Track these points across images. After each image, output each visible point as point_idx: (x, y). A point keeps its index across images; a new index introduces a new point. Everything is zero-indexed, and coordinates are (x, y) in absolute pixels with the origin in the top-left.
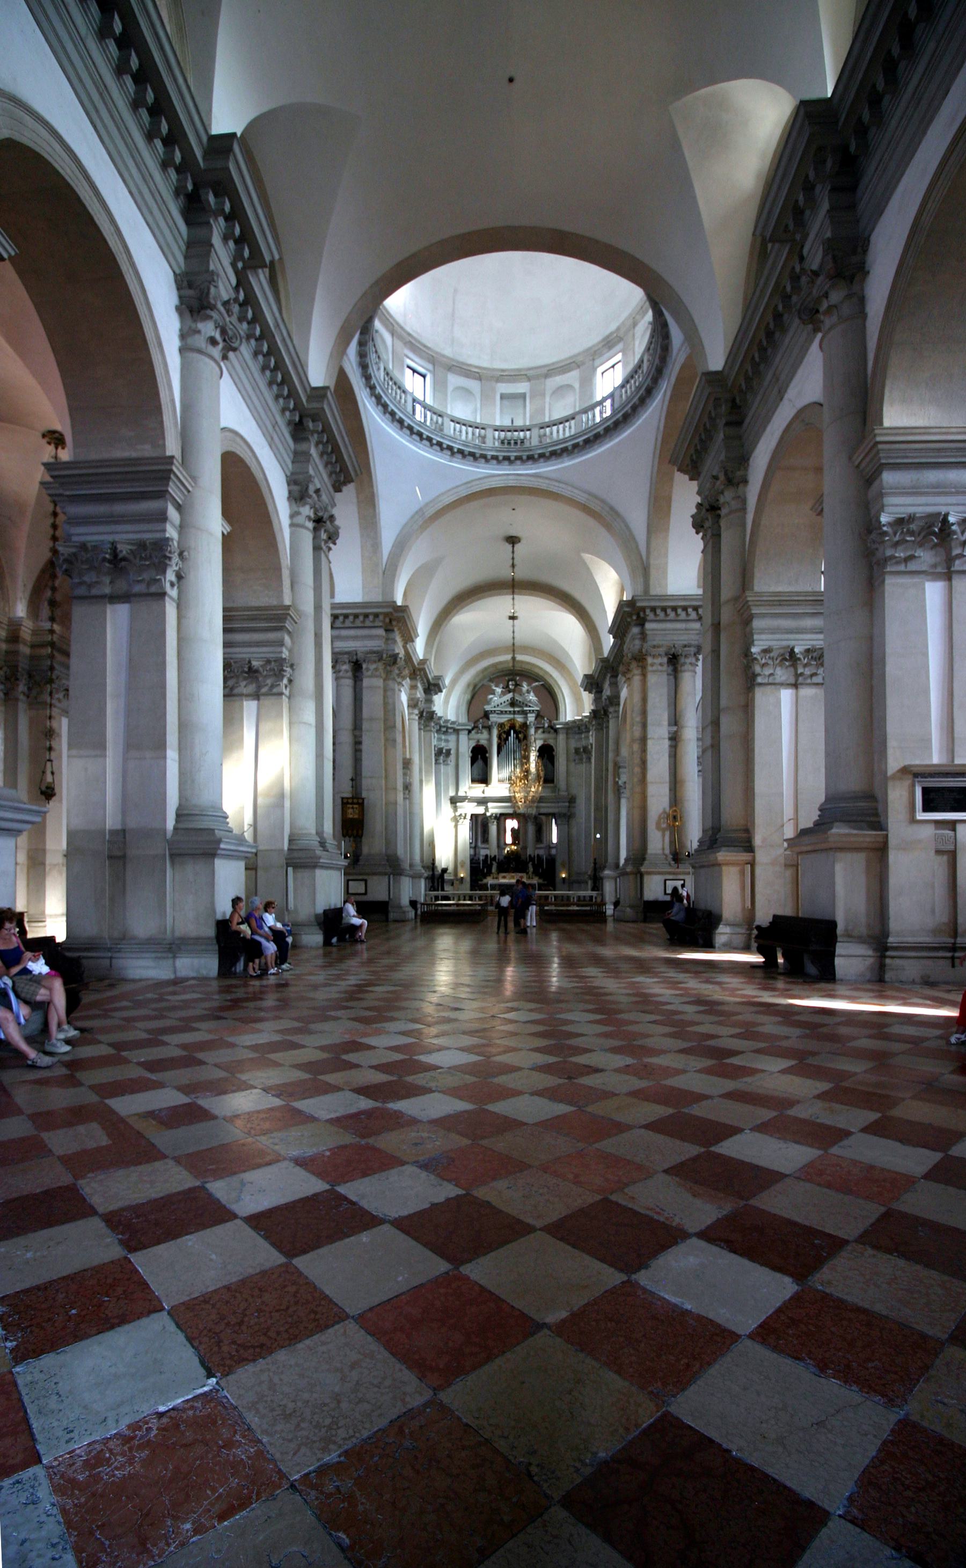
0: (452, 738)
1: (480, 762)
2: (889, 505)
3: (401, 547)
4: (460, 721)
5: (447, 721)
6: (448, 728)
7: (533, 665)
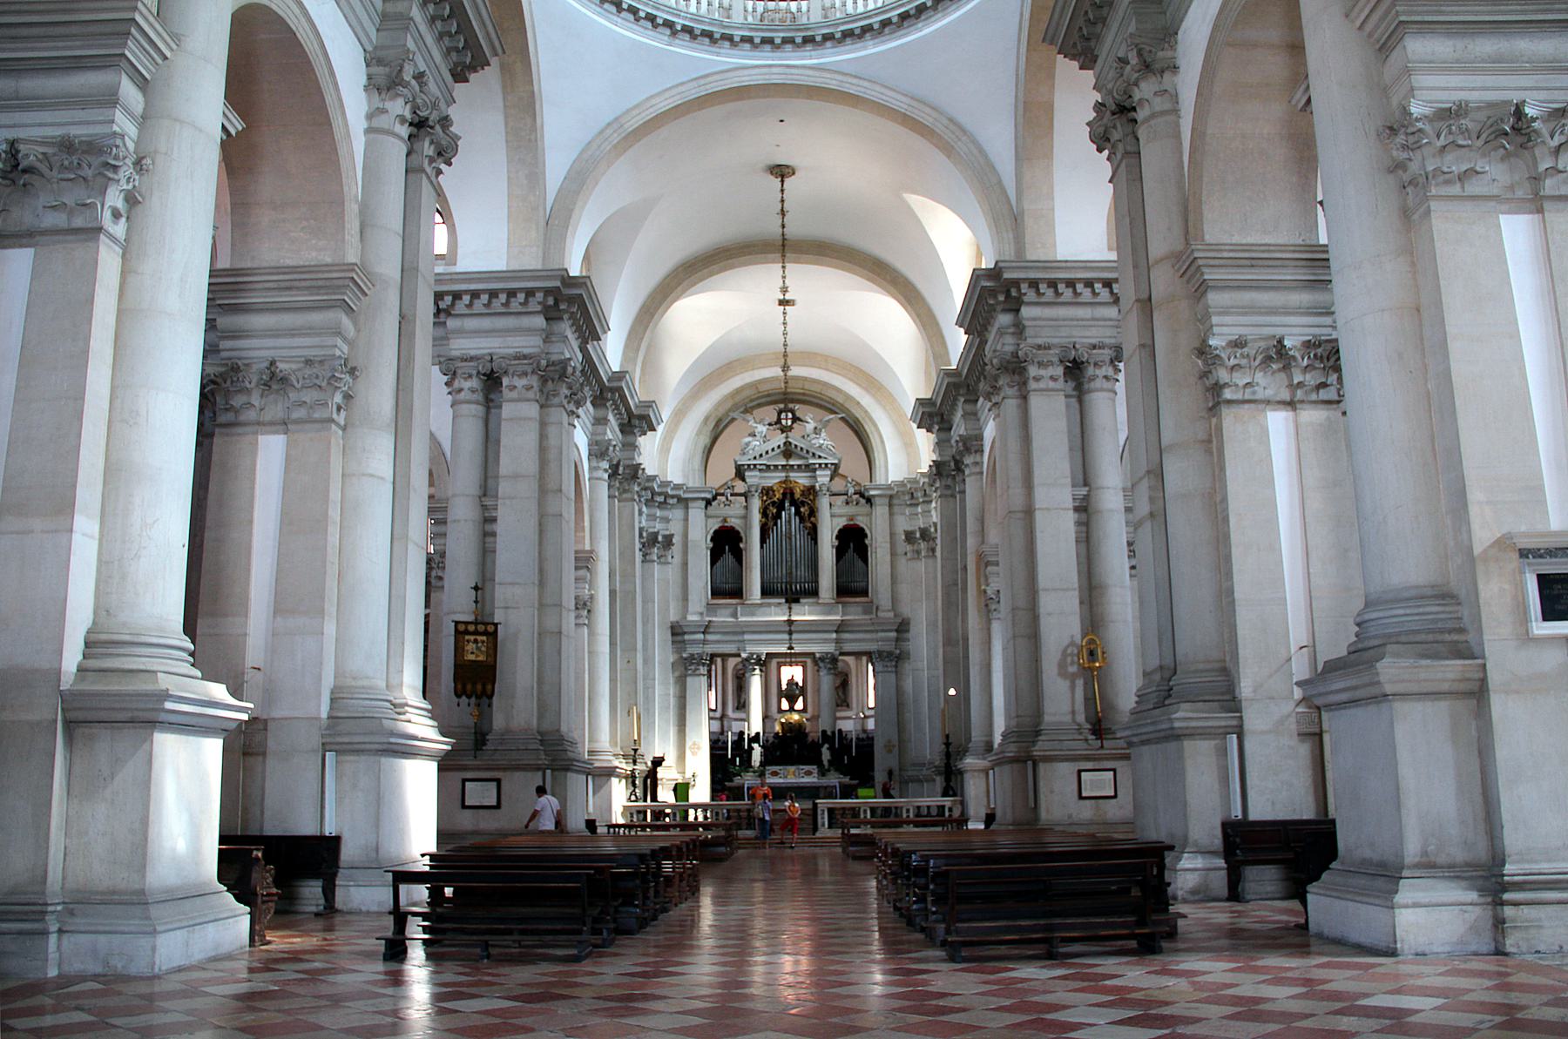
0: (676, 514)
1: (728, 558)
2: (1421, 89)
3: (580, 179)
4: (690, 485)
5: (666, 484)
6: (666, 496)
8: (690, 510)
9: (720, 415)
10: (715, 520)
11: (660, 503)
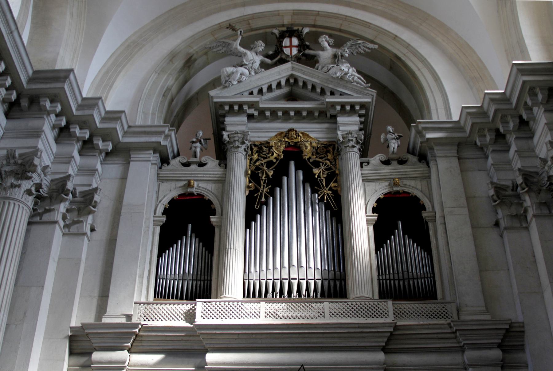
7: (346, 18)
8: (131, 163)
10: (173, 185)
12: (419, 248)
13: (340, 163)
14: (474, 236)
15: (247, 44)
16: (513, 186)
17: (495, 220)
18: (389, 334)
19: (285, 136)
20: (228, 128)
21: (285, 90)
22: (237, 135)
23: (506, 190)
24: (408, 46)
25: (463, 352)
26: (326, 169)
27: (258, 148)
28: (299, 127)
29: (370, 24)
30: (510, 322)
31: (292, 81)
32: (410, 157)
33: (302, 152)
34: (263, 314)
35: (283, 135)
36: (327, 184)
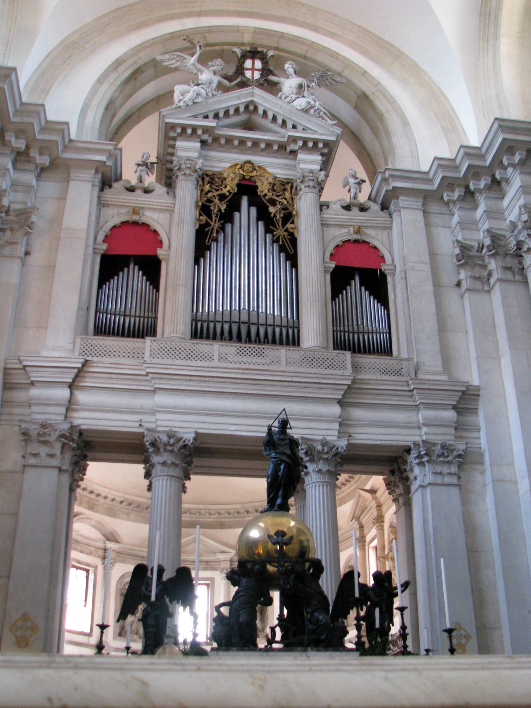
7: (312, 45)
8: (72, 183)
9: (141, 63)
11: (19, 154)
12: (376, 301)
13: (298, 203)
14: (435, 294)
15: (204, 60)
16: (478, 248)
17: (457, 280)
18: (346, 387)
19: (241, 168)
20: (180, 153)
21: (243, 117)
22: (188, 162)
23: (470, 251)
24: (377, 84)
25: (418, 411)
26: (284, 209)
27: (211, 178)
28: (257, 159)
29: (339, 54)
30: (466, 384)
31: (251, 108)
32: (371, 204)
33: (257, 187)
34: (216, 358)
35: (238, 167)
36: (284, 225)
